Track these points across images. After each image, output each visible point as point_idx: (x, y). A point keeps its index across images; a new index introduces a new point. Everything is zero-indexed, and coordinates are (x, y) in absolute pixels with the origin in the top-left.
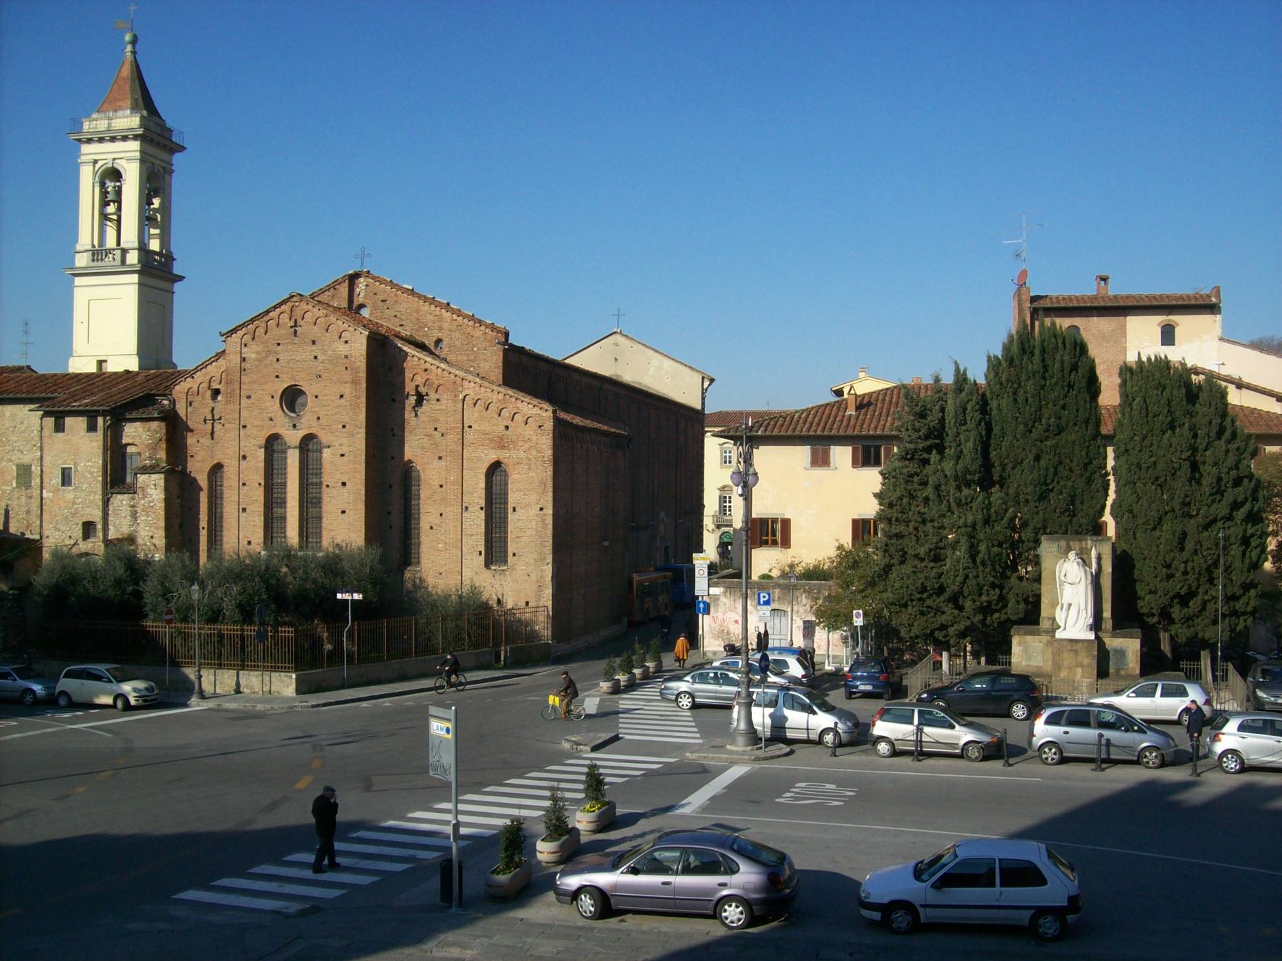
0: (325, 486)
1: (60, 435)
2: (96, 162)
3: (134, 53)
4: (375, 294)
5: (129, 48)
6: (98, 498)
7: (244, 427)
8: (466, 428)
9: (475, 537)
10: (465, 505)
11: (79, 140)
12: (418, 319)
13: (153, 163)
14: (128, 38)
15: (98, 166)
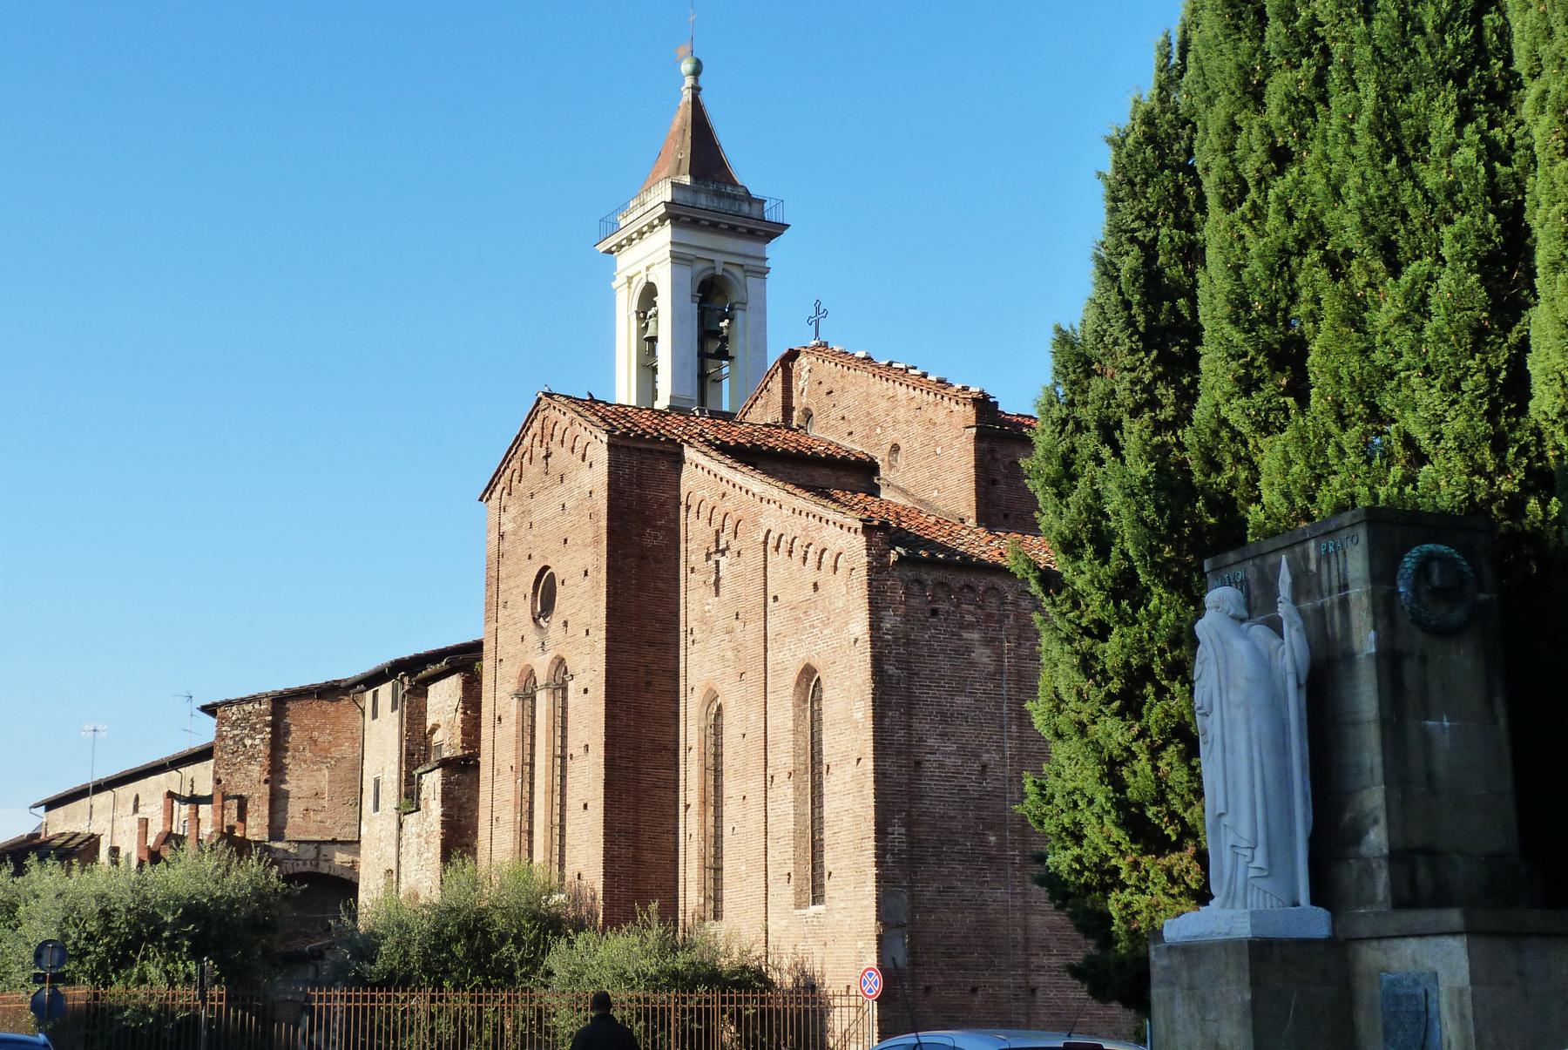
0: (569, 758)
1: (376, 721)
2: (630, 279)
3: (696, 90)
4: (820, 383)
5: (689, 81)
6: (395, 824)
7: (501, 660)
8: (770, 600)
9: (782, 842)
10: (770, 771)
11: (609, 252)
12: (868, 413)
13: (713, 261)
14: (686, 67)
15: (633, 285)
